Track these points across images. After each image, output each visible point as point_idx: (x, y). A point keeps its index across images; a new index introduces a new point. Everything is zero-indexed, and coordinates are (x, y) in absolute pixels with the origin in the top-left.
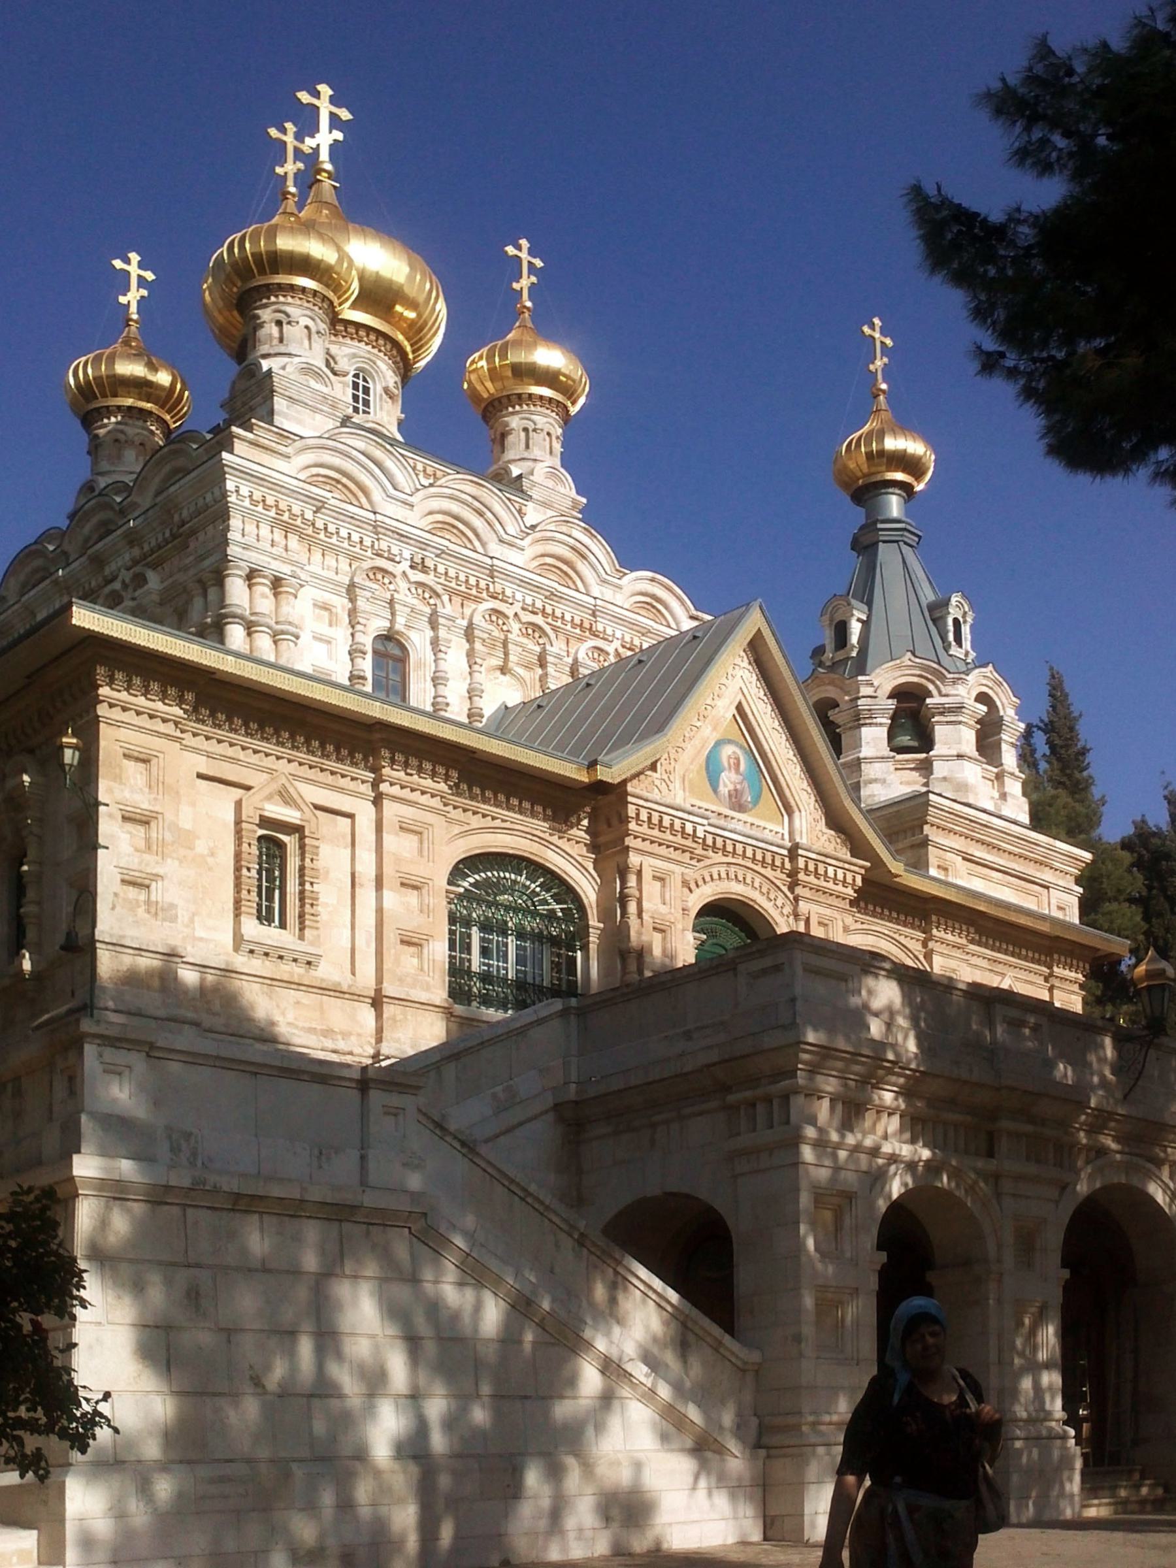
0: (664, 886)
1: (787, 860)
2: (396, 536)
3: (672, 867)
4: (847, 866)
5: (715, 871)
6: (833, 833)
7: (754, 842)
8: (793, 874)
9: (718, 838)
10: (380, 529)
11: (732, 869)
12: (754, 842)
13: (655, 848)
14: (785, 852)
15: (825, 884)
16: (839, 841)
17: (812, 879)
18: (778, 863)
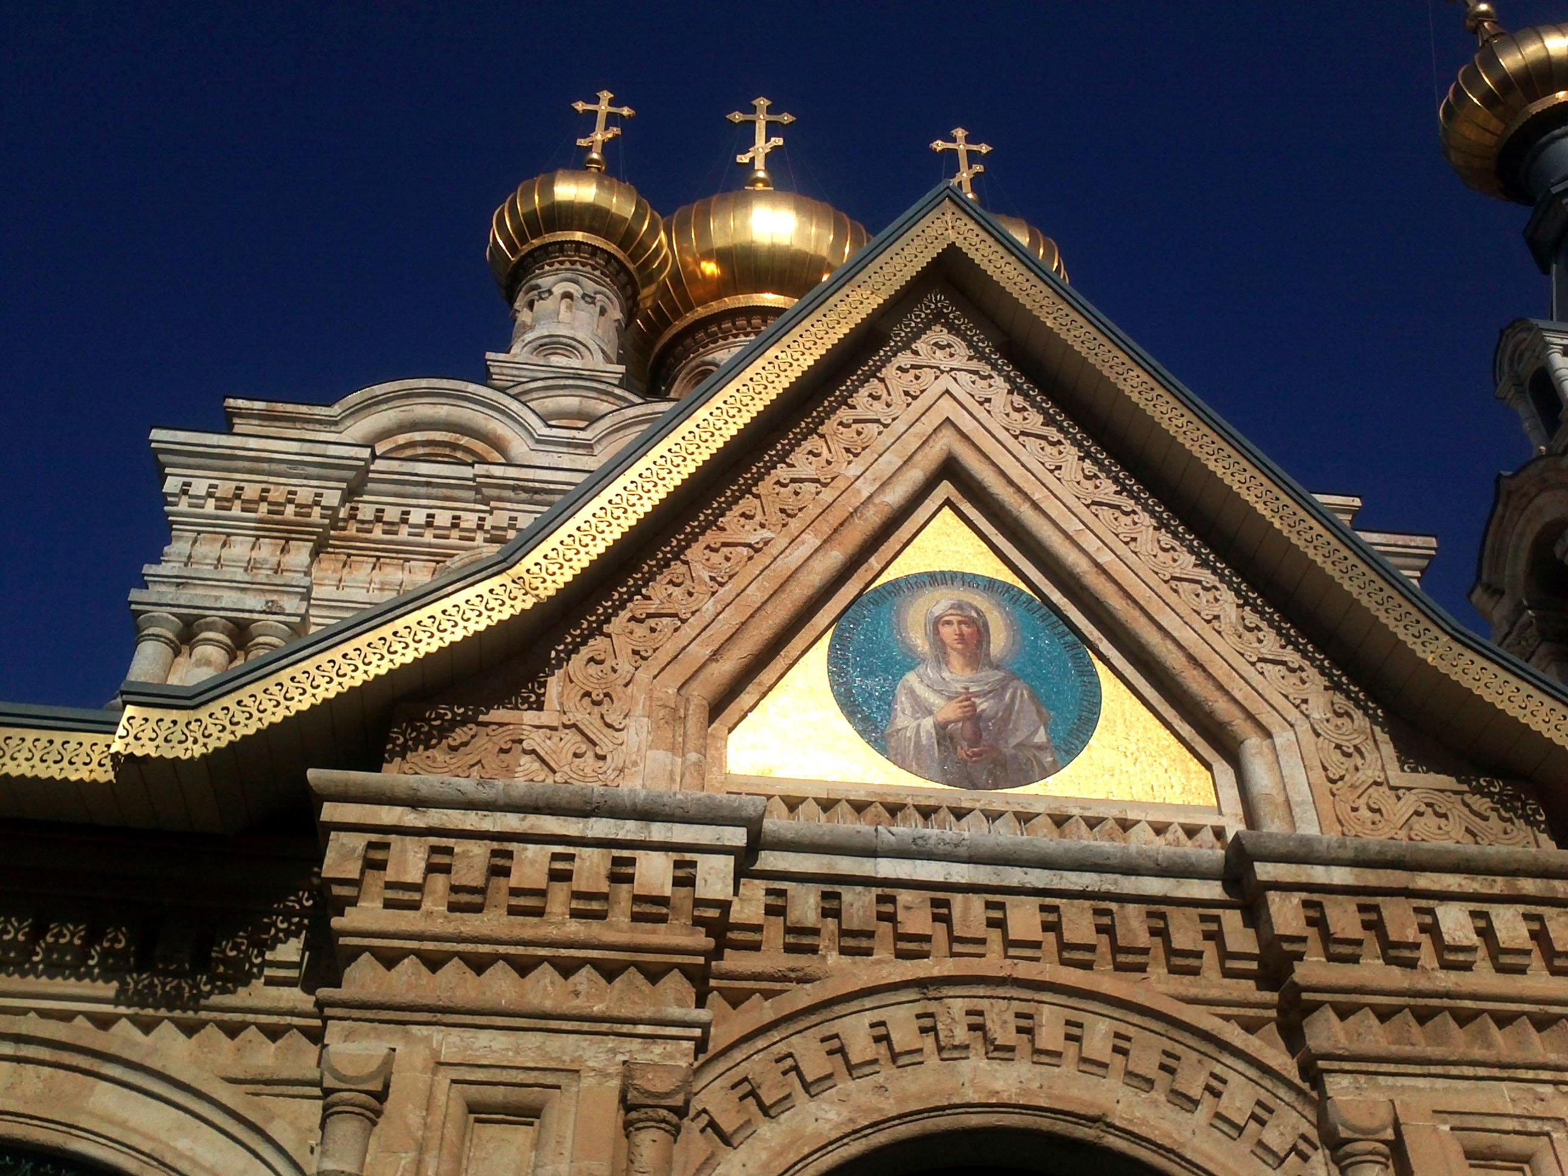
0: (537, 1145)
1: (1232, 919)
2: (524, 496)
3: (564, 1047)
4: (1529, 886)
5: (855, 1030)
6: (1447, 781)
7: (1038, 878)
8: (1274, 965)
9: (848, 895)
10: (486, 491)
11: (956, 1007)
12: (1038, 878)
13: (454, 983)
14: (1213, 890)
15: (1448, 980)
16: (1481, 804)
17: (1371, 970)
18: (1185, 933)
